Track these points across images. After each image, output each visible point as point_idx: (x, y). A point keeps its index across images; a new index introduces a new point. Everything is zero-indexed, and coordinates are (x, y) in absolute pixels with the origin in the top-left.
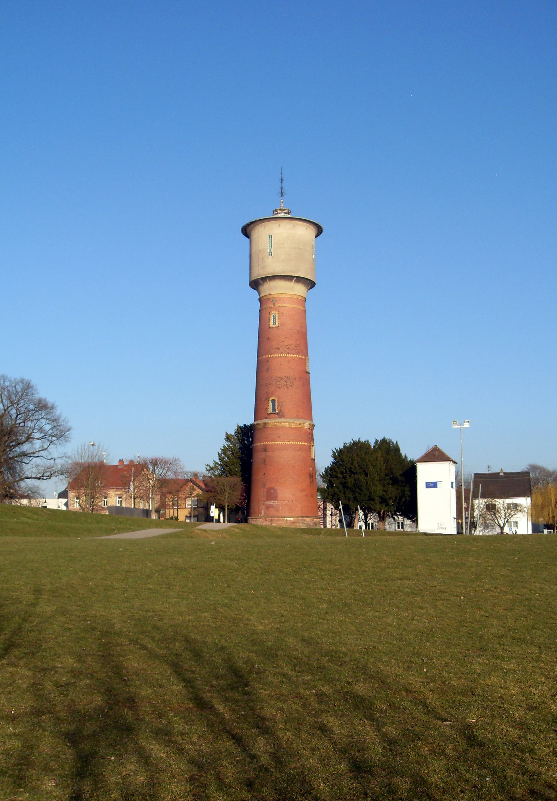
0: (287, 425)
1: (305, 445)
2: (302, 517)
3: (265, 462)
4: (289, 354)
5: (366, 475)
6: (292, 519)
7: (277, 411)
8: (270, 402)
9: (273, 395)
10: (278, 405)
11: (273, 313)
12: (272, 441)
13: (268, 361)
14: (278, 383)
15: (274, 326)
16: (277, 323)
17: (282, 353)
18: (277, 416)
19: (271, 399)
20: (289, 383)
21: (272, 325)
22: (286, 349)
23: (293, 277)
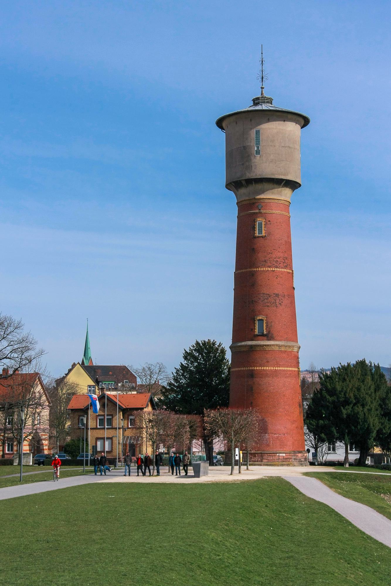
0: (277, 348)
1: (295, 371)
2: (295, 452)
3: (252, 390)
4: (277, 267)
5: (363, 406)
6: (284, 455)
7: (265, 333)
8: (257, 322)
9: (260, 314)
10: (267, 326)
11: (259, 220)
12: (261, 366)
13: (253, 275)
14: (266, 301)
15: (260, 235)
16: (263, 232)
17: (270, 267)
18: (265, 338)
19: (258, 318)
20: (278, 301)
21: (257, 234)
22: (274, 263)
23: (282, 180)
